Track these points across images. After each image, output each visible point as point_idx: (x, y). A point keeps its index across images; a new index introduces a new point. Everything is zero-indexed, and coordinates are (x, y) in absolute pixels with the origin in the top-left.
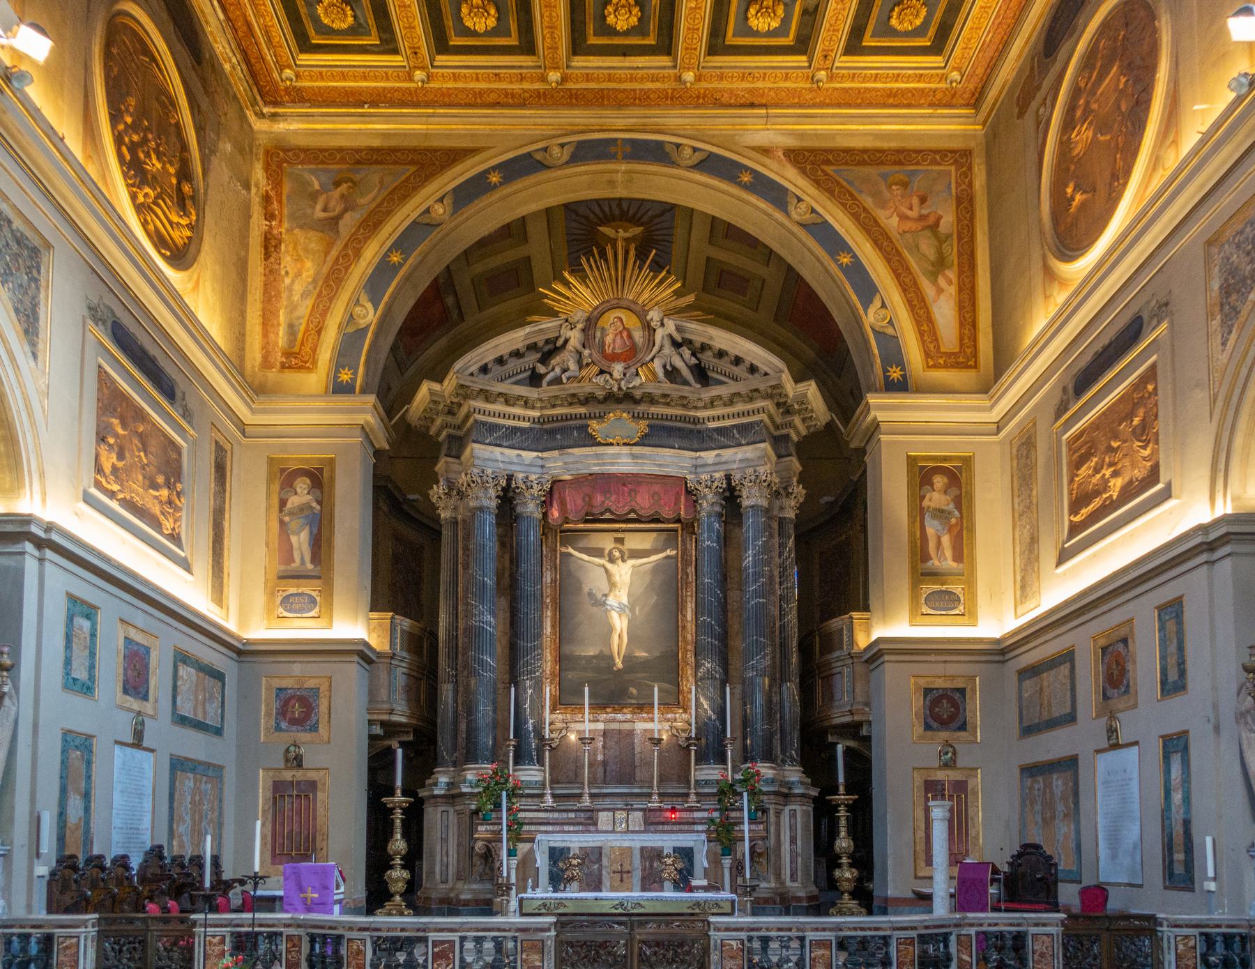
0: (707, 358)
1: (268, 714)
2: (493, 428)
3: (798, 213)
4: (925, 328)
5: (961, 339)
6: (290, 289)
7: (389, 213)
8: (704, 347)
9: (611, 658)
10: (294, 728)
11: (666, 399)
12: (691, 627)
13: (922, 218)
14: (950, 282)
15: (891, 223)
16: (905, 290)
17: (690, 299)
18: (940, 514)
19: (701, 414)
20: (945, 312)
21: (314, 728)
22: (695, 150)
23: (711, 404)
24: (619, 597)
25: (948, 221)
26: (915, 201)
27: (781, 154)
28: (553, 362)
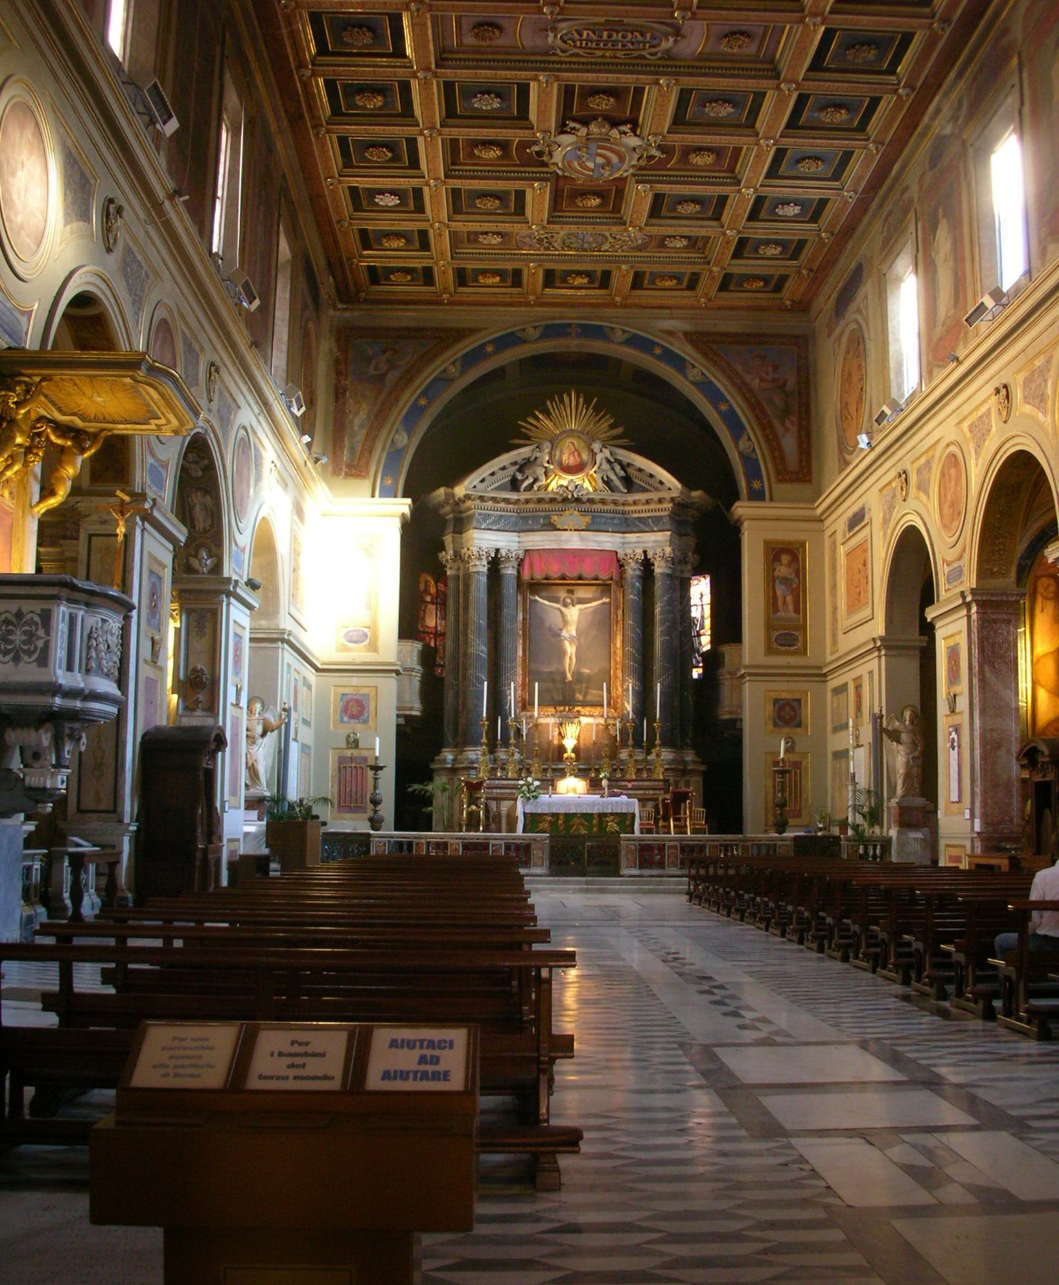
0: (630, 470)
1: (335, 711)
2: (486, 517)
3: (693, 374)
4: (777, 454)
5: (801, 461)
6: (352, 422)
7: (419, 371)
8: (629, 465)
9: (564, 674)
10: (353, 721)
11: (603, 502)
12: (619, 652)
13: (774, 380)
14: (793, 425)
15: (756, 383)
16: (763, 429)
17: (620, 430)
18: (785, 581)
19: (627, 508)
20: (789, 443)
21: (366, 722)
22: (624, 332)
23: (635, 503)
24: (572, 630)
25: (792, 382)
26: (770, 369)
27: (681, 335)
28: (527, 472)
